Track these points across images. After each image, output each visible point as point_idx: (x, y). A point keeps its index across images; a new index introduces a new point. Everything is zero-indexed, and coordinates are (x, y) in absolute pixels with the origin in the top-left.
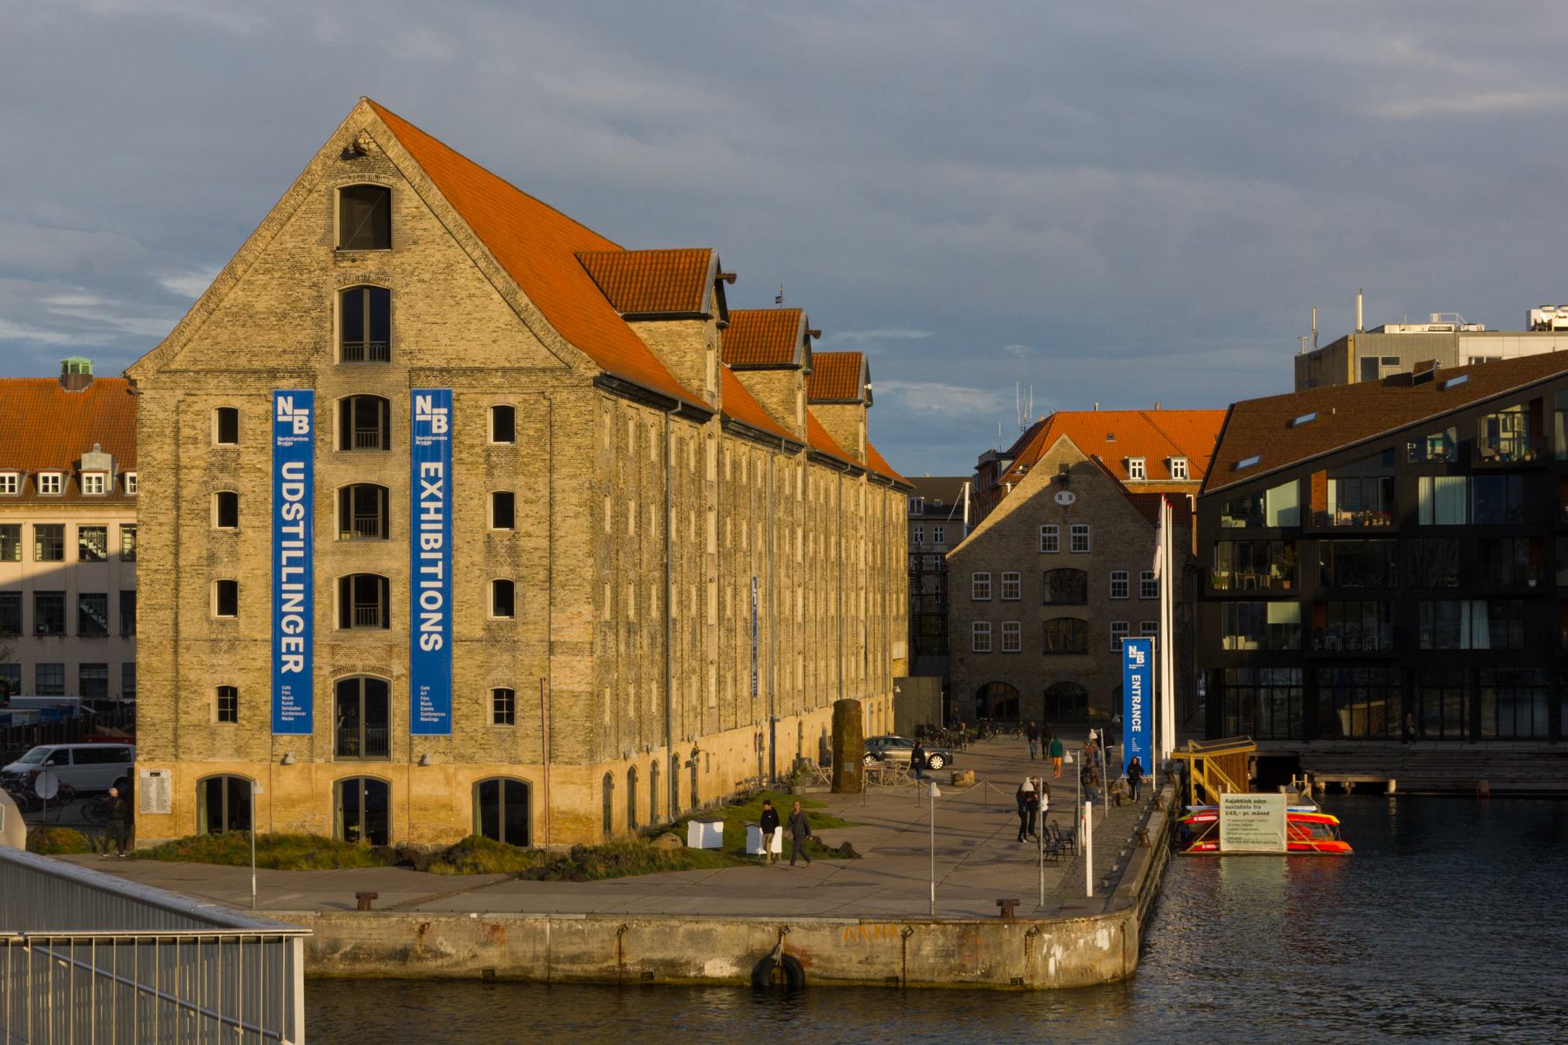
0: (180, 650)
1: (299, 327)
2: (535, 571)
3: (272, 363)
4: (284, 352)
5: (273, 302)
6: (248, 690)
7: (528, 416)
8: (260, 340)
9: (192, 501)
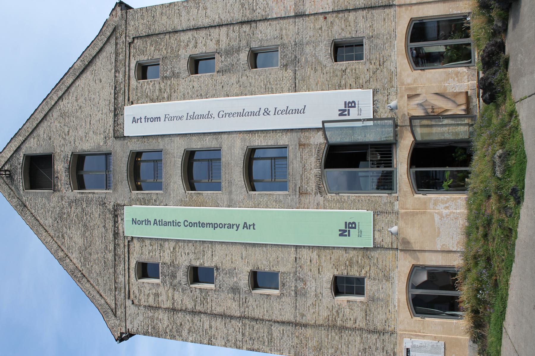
0: (304, 322)
1: (91, 216)
2: (244, 34)
3: (111, 236)
4: (104, 226)
5: (78, 233)
6: (336, 267)
7: (143, 53)
8: (98, 244)
9: (195, 301)
